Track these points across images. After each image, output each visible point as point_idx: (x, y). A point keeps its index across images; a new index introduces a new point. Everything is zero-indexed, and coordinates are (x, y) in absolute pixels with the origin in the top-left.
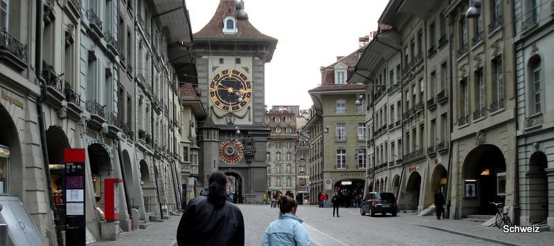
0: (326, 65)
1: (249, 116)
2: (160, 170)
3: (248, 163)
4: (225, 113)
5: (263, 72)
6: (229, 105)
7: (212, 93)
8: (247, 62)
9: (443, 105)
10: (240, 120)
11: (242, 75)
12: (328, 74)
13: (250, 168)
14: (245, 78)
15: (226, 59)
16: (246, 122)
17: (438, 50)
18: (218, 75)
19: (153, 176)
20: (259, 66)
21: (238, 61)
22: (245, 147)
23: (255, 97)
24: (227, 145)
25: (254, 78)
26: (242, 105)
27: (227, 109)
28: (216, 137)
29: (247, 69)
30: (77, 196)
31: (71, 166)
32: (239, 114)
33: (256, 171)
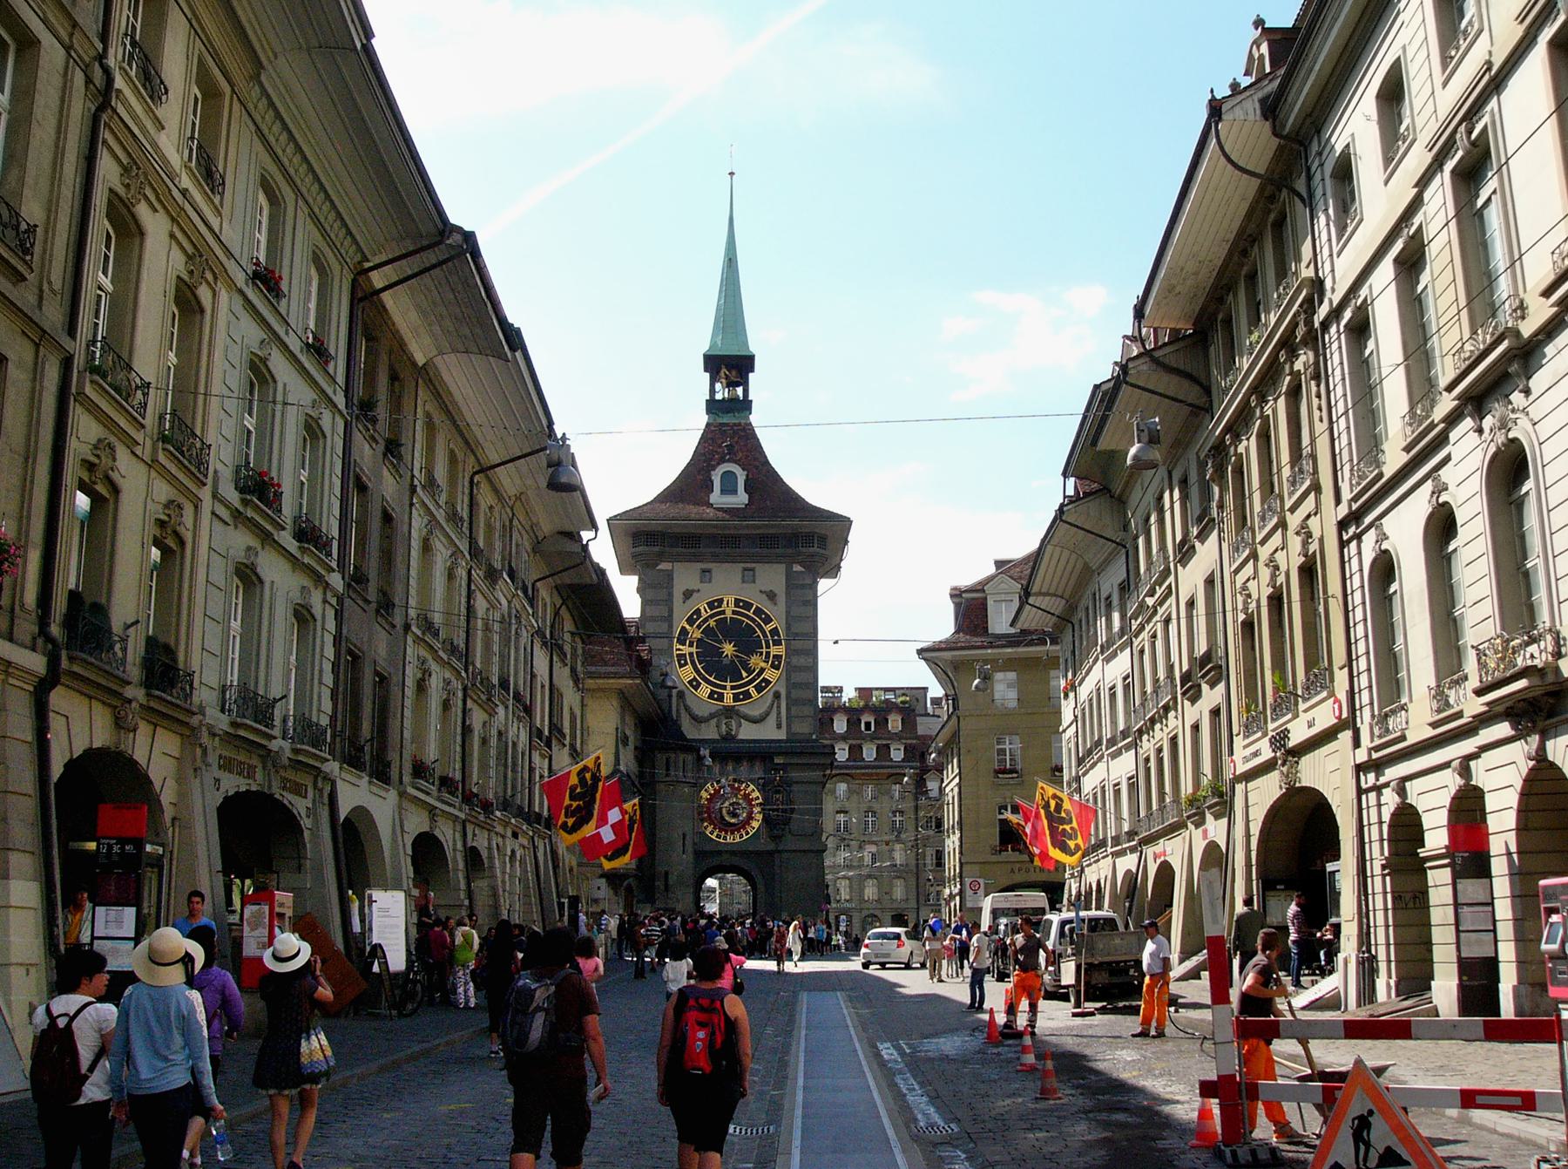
0: (968, 579)
1: (779, 713)
2: (491, 858)
3: (776, 838)
5: (812, 604)
6: (724, 688)
8: (772, 576)
9: (1213, 685)
11: (758, 611)
12: (971, 608)
16: (770, 732)
17: (1197, 544)
19: (461, 876)
20: (803, 586)
25: (790, 620)
26: (759, 689)
27: (721, 698)
29: (771, 596)
30: (119, 923)
31: (110, 847)
32: (744, 707)
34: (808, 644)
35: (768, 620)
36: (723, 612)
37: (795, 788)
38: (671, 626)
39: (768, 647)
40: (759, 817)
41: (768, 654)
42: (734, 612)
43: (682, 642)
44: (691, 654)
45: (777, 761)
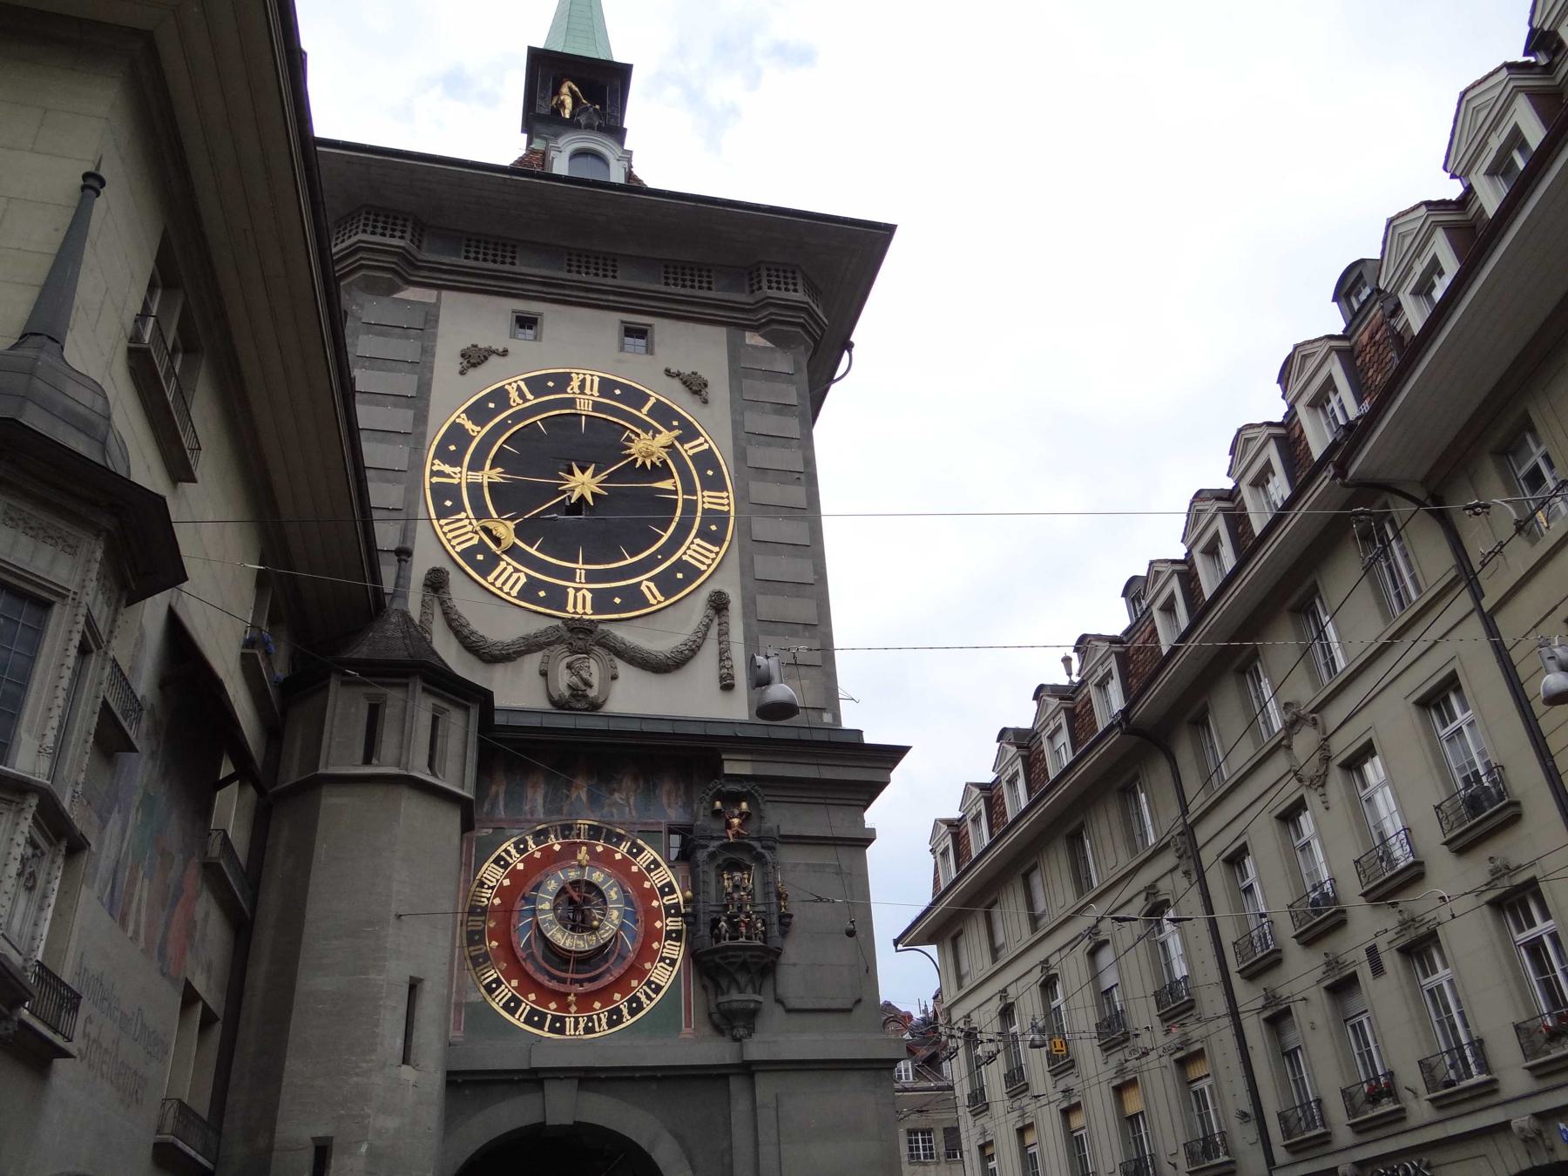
1: (724, 656)
4: (537, 626)
6: (570, 575)
13: (748, 1070)
14: (689, 433)
16: (697, 699)
18: (501, 396)
20: (773, 375)
22: (695, 883)
23: (751, 545)
24: (538, 867)
25: (743, 439)
26: (667, 584)
27: (557, 598)
29: (696, 387)
32: (628, 635)
33: (810, 1103)
34: (796, 495)
35: (689, 433)
36: (571, 403)
38: (421, 418)
39: (689, 488)
40: (675, 951)
41: (690, 507)
42: (597, 406)
43: (455, 460)
44: (475, 489)
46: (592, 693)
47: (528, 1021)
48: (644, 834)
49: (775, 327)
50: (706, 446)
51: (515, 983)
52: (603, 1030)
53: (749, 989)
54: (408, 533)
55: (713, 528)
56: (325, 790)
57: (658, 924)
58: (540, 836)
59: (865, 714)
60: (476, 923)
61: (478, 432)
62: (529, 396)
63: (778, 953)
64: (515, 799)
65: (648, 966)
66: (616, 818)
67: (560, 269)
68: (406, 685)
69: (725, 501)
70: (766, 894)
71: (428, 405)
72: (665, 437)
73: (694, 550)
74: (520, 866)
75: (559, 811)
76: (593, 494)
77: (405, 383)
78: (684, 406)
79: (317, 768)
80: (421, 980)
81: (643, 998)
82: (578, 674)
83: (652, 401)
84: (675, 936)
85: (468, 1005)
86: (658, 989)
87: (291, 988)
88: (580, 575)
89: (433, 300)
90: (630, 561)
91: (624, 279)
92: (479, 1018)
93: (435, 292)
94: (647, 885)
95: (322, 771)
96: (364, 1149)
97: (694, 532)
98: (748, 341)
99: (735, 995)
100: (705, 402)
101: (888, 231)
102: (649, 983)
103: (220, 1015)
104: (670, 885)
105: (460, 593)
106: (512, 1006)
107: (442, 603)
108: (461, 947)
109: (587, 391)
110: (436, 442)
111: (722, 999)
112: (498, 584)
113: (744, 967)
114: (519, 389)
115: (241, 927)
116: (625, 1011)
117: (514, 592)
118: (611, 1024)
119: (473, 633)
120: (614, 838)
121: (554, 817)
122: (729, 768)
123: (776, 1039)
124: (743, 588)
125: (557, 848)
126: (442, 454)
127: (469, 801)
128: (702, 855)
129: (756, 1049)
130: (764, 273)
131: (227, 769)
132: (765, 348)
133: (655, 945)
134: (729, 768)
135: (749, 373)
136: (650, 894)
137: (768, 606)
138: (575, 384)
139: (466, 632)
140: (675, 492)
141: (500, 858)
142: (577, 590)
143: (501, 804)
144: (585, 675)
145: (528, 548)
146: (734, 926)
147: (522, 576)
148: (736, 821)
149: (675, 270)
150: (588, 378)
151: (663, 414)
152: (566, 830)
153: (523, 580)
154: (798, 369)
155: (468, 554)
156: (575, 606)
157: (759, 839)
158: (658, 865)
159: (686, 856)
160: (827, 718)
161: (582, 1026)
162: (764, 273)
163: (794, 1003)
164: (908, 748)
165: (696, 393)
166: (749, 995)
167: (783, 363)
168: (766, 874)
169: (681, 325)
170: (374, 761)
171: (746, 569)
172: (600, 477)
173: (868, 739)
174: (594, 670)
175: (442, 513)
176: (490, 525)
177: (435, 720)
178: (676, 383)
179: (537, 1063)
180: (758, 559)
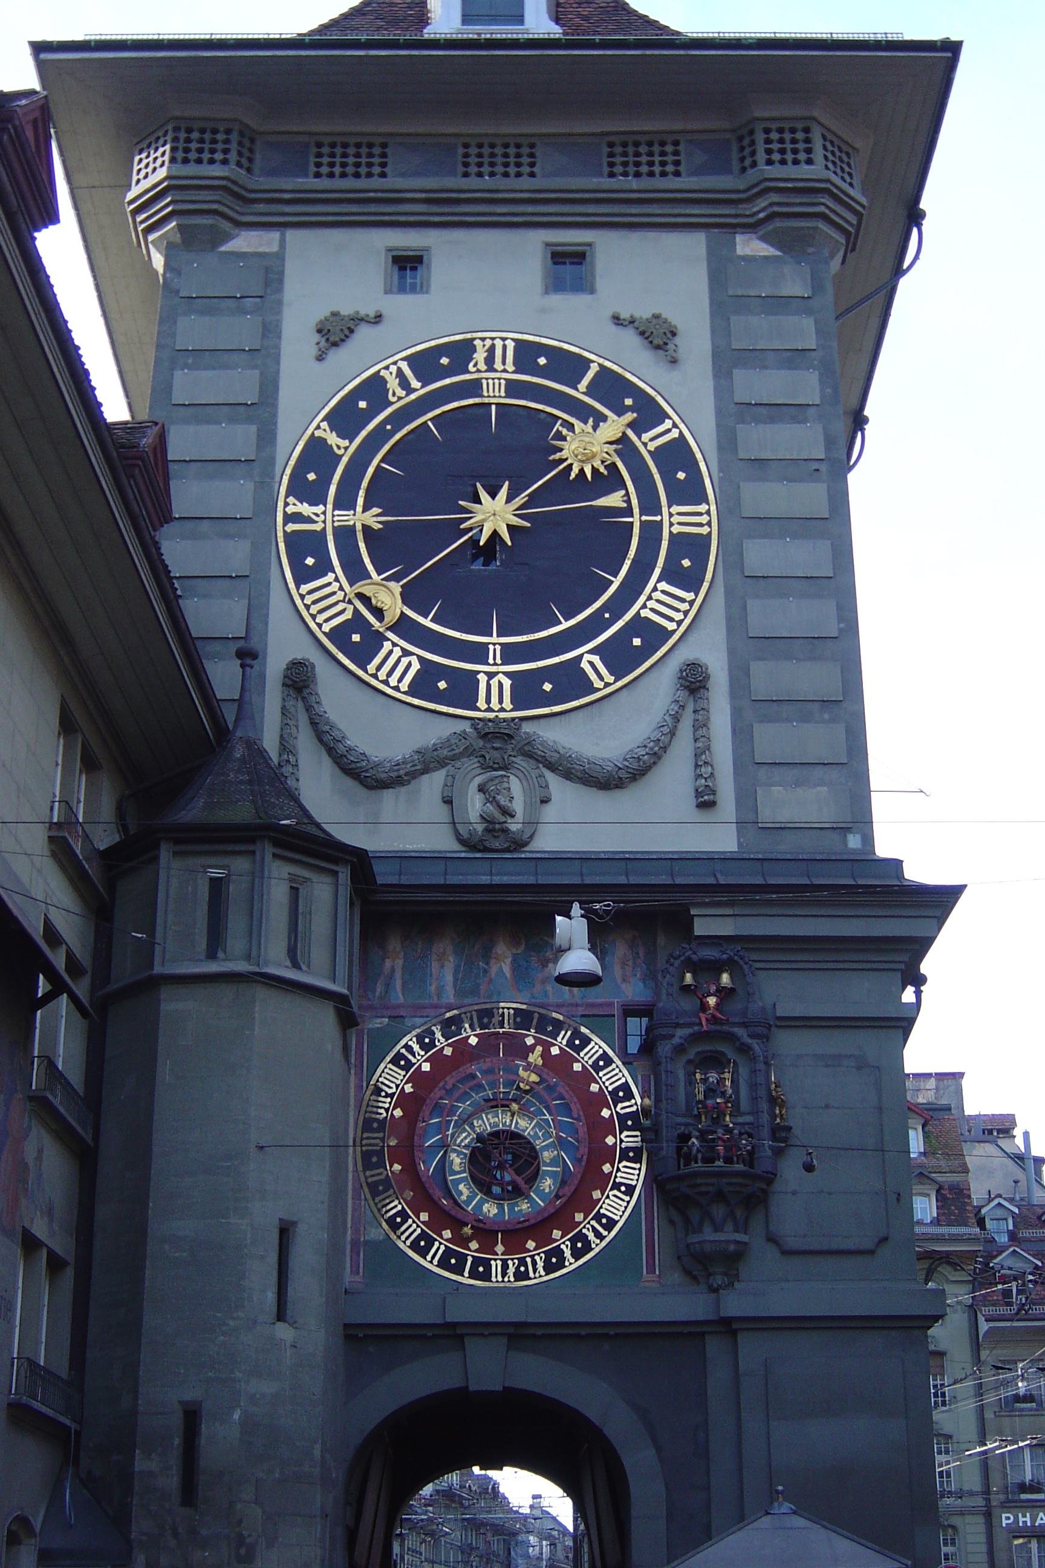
1: (701, 757)
6: (479, 654)
7: (305, 548)
8: (658, 273)
10: (603, 804)
13: (729, 1327)
14: (649, 414)
15: (451, 254)
18: (374, 388)
21: (569, 268)
23: (745, 585)
25: (735, 414)
26: (619, 657)
27: (463, 690)
28: (319, 955)
29: (658, 337)
32: (567, 733)
36: (474, 387)
37: (787, 1042)
38: (267, 436)
39: (650, 505)
40: (633, 1173)
41: (652, 532)
42: (514, 389)
43: (316, 496)
44: (345, 534)
45: (707, 925)
46: (514, 827)
47: (443, 1263)
48: (589, 1018)
49: (778, 223)
50: (675, 433)
51: (424, 1217)
52: (539, 1276)
53: (729, 1226)
54: (257, 612)
55: (686, 563)
56: (165, 992)
57: (610, 1140)
58: (451, 1026)
59: (908, 837)
60: (374, 1139)
61: (345, 448)
62: (415, 384)
63: (770, 1177)
64: (416, 975)
65: (596, 1194)
66: (552, 999)
67: (452, 173)
68: (253, 853)
69: (704, 519)
70: (754, 1099)
71: (274, 415)
72: (614, 426)
73: (659, 601)
74: (426, 1067)
75: (474, 991)
76: (510, 527)
77: (240, 384)
78: (640, 369)
79: (151, 966)
80: (294, 1224)
81: (591, 1236)
82: (494, 801)
83: (594, 368)
84: (632, 1155)
85: (366, 1243)
86: (610, 1224)
87: (142, 1229)
88: (494, 653)
89: (275, 248)
90: (565, 625)
91: (550, 176)
92: (384, 1260)
93: (275, 235)
94: (594, 1088)
95: (158, 969)
96: (236, 1416)
97: (657, 572)
98: (740, 251)
99: (709, 1235)
100: (674, 361)
101: (951, 49)
102: (598, 1217)
103: (71, 1258)
104: (625, 1087)
105: (334, 695)
106: (422, 1245)
107: (308, 709)
108: (356, 1170)
109: (498, 365)
110: (288, 471)
111: (694, 1239)
112: (382, 675)
113: (720, 1196)
114: (400, 373)
115: (85, 1157)
116: (568, 1253)
117: (404, 686)
118: (549, 1268)
119: (350, 749)
120: (549, 1027)
121: (467, 1001)
122: (701, 928)
123: (768, 1288)
124: (732, 652)
125: (473, 1041)
126: (300, 489)
127: (339, 1001)
128: (664, 1049)
129: (734, 1305)
130: (760, 137)
131: (43, 986)
132: (766, 257)
133: (607, 1168)
134: (701, 928)
135: (742, 304)
136: (600, 1101)
137: (766, 677)
138: (480, 356)
139: (341, 749)
140: (629, 511)
141: (399, 1056)
142: (491, 675)
143: (398, 983)
144: (502, 800)
145: (420, 619)
146: (709, 1145)
147: (414, 660)
148: (712, 1001)
149: (625, 153)
150: (499, 344)
151: (612, 388)
152: (485, 1017)
153: (416, 666)
154: (817, 286)
155: (339, 635)
156: (488, 700)
157: (744, 1025)
158: (609, 1061)
159: (648, 1047)
160: (854, 842)
161: (511, 1270)
162: (760, 137)
163: (792, 1243)
164: (962, 888)
165: (658, 347)
166: (729, 1235)
167: (795, 285)
168: (754, 1072)
169: (636, 238)
170: (221, 955)
171: (736, 623)
172: (519, 501)
173: (914, 873)
174: (516, 792)
175: (303, 575)
176: (367, 591)
177: (295, 890)
178: (630, 338)
179: (456, 1314)
180: (754, 605)
